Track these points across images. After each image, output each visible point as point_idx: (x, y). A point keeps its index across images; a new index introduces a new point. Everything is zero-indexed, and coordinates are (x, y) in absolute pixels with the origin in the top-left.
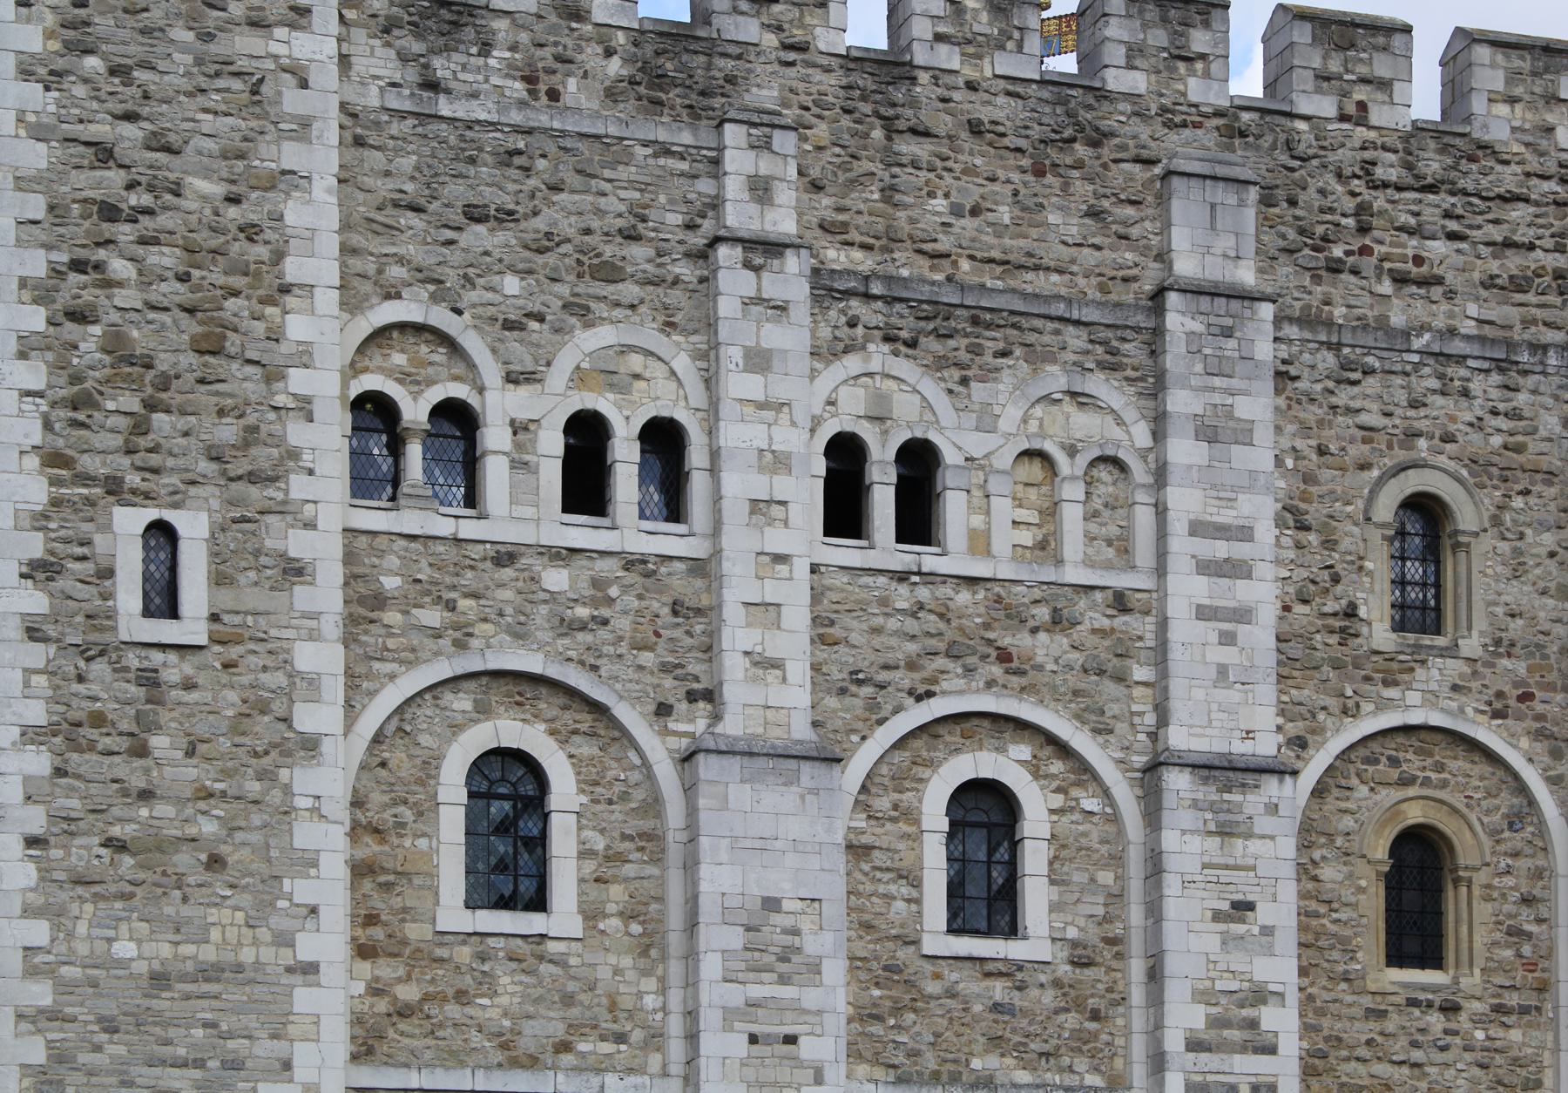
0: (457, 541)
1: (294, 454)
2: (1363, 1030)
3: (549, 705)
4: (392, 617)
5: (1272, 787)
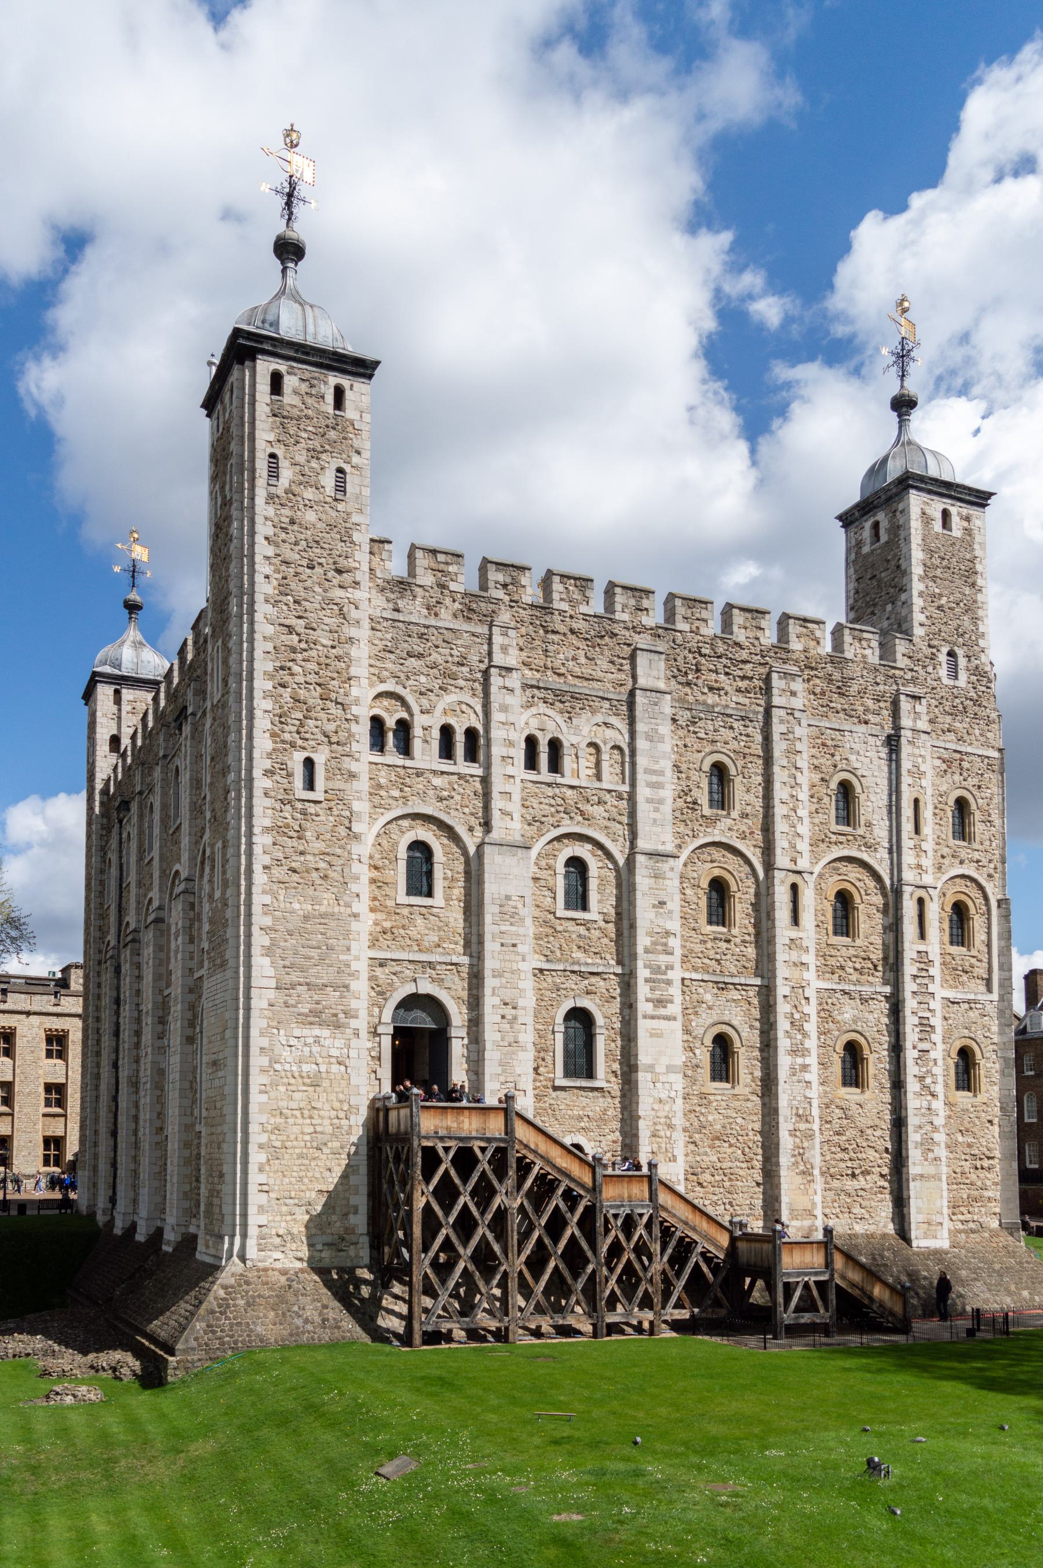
0: (404, 767)
4: (383, 793)
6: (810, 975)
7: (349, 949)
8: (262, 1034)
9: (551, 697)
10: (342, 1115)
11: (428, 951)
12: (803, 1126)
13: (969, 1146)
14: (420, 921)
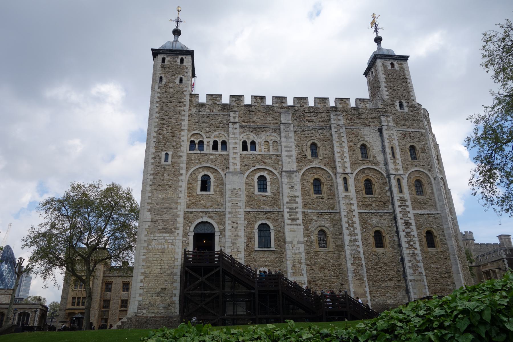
1: (181, 145)
2: (311, 201)
3: (211, 170)
4: (193, 162)
5: (295, 174)
6: (355, 207)
7: (177, 208)
8: (145, 236)
9: (251, 130)
10: (172, 262)
11: (208, 208)
12: (357, 262)
13: (437, 268)
14: (205, 199)
